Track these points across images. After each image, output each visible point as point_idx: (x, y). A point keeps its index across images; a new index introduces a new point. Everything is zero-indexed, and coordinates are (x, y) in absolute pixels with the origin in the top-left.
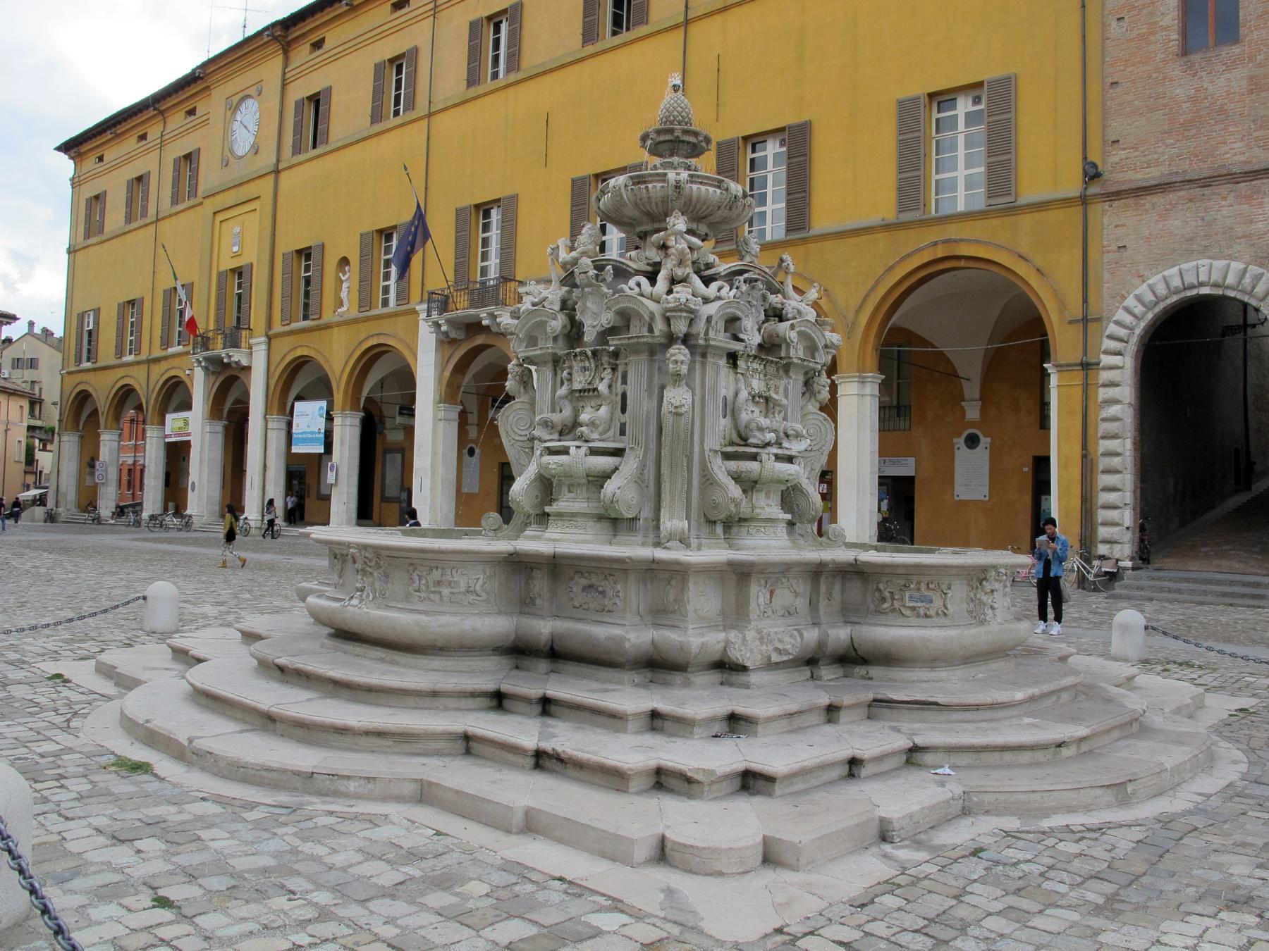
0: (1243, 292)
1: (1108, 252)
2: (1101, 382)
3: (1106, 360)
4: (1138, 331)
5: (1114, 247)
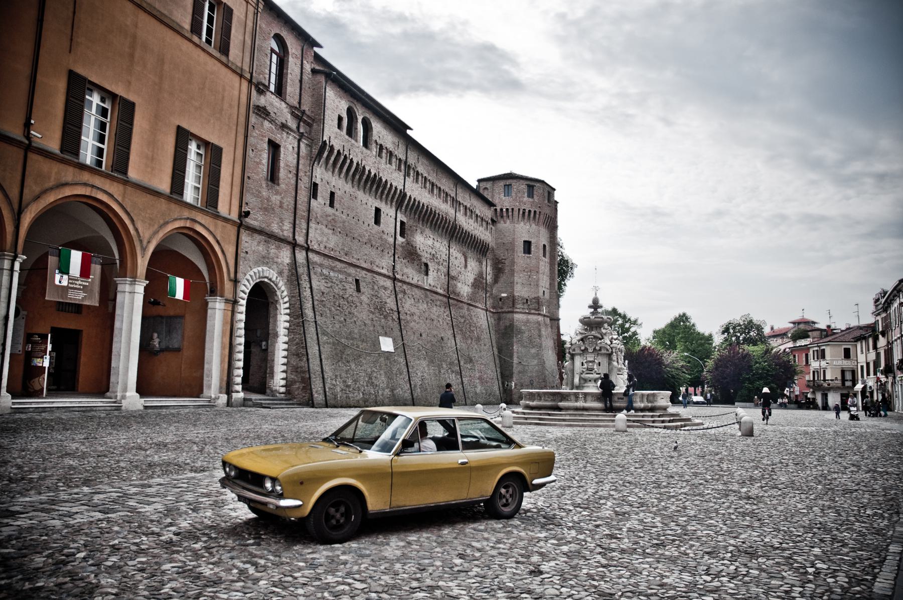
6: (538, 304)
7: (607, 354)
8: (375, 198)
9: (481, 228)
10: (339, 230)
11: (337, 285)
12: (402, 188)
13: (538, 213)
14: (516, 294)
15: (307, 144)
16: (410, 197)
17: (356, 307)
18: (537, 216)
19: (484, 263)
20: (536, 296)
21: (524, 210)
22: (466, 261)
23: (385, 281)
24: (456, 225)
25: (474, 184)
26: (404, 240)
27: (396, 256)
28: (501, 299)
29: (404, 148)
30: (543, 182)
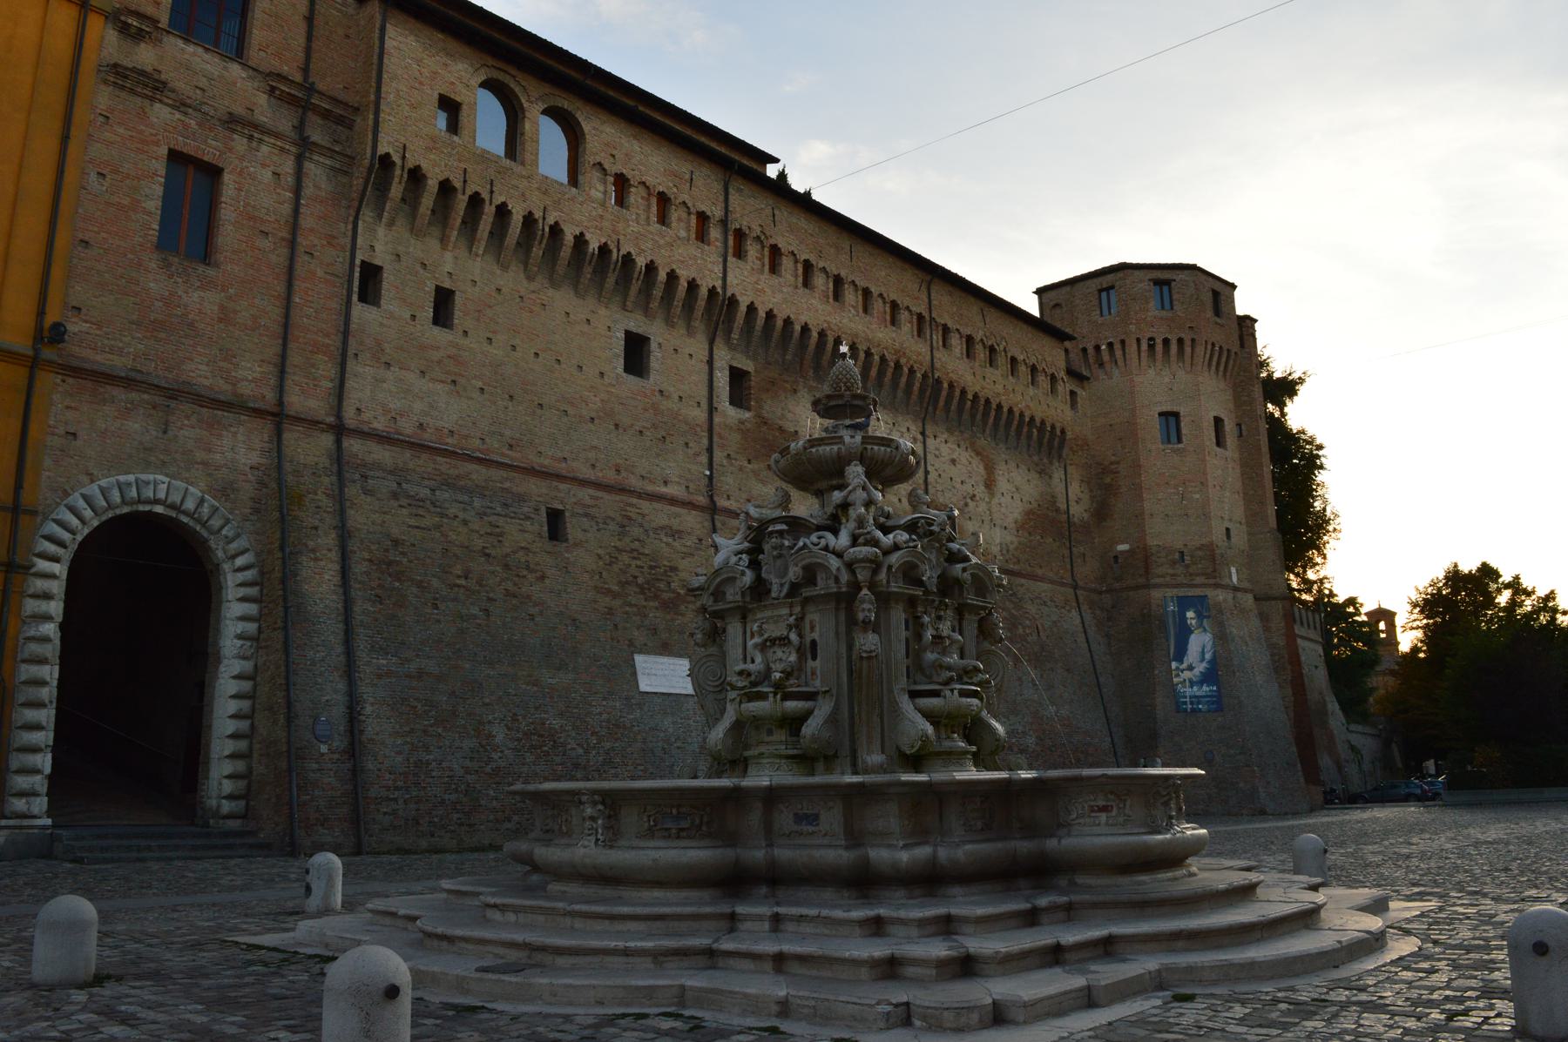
0: (198, 521)
1: (53, 434)
2: (31, 591)
3: (43, 565)
4: (79, 538)
5: (61, 431)
6: (1214, 560)
7: (838, 597)
8: (624, 308)
9: (1031, 391)
10: (480, 384)
11: (465, 522)
12: (718, 284)
13: (1188, 343)
14: (1152, 542)
15: (332, 168)
16: (752, 308)
17: (543, 578)
18: (1188, 350)
19: (1058, 475)
20: (1204, 541)
21: (1151, 339)
22: (990, 469)
23: (677, 515)
24: (938, 382)
25: (1032, 306)
26: (747, 415)
27: (719, 455)
28: (1116, 558)
29: (717, 187)
30: (1193, 268)
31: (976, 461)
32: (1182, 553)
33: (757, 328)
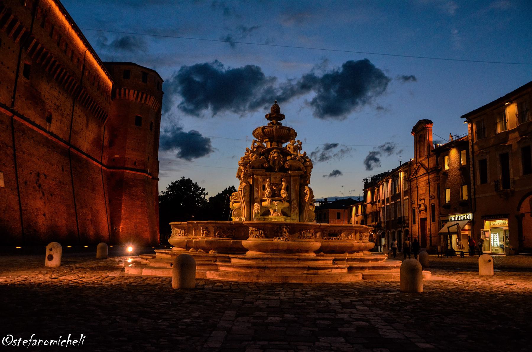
22: (88, 122)
26: (27, 81)
27: (17, 95)
28: (114, 160)
31: (85, 118)
32: (135, 162)
33: (37, 48)
